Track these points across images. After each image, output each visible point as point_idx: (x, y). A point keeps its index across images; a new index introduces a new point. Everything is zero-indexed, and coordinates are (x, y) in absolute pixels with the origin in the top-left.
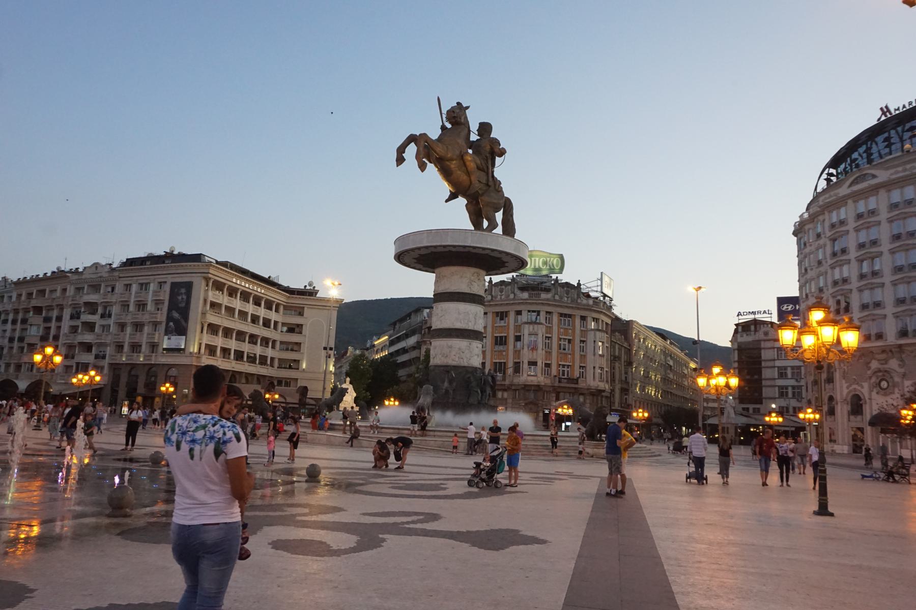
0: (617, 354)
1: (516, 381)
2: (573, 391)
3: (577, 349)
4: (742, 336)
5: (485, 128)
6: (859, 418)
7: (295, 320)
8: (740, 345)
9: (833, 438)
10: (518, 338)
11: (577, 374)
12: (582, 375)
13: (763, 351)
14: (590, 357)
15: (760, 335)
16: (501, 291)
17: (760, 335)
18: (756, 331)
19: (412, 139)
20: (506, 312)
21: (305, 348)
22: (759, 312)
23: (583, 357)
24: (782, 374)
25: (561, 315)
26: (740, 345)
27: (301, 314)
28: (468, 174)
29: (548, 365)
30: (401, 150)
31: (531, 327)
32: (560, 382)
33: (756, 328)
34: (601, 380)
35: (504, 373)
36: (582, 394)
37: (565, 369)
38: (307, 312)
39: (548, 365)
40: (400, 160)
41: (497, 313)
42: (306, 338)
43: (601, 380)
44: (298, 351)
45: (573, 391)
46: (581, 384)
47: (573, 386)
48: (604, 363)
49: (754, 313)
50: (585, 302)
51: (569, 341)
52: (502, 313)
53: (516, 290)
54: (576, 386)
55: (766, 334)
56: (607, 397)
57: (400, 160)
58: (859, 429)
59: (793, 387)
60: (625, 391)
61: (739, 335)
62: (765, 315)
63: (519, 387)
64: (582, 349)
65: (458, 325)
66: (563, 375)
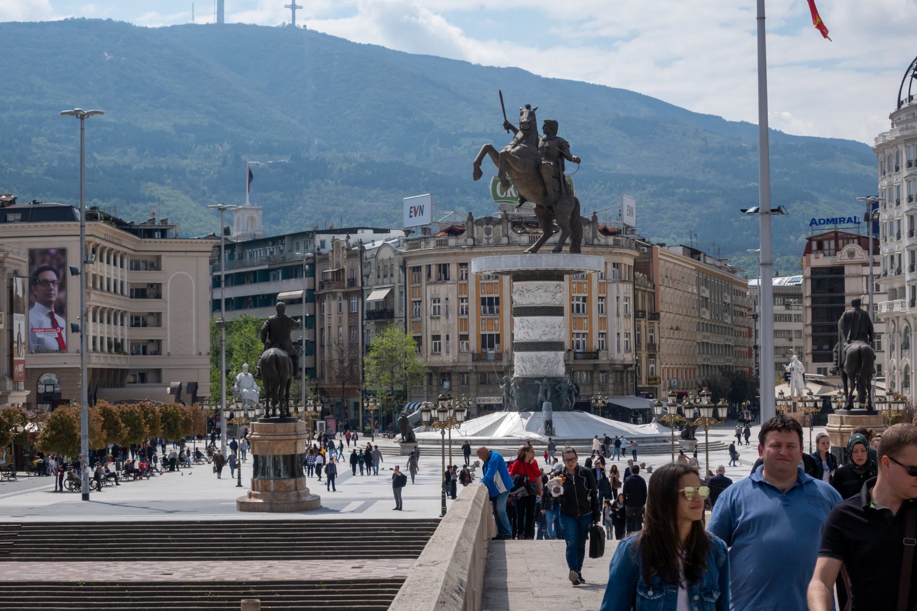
0: (640, 308)
3: (595, 310)
4: (817, 258)
5: (551, 127)
7: (146, 277)
8: (814, 270)
11: (595, 345)
12: (603, 346)
13: (847, 281)
14: (612, 320)
15: (842, 257)
16: (488, 232)
17: (842, 257)
18: (837, 249)
19: (489, 149)
21: (167, 320)
22: (842, 220)
23: (603, 321)
26: (814, 270)
27: (155, 265)
30: (478, 163)
32: (575, 358)
33: (837, 244)
34: (628, 350)
36: (603, 372)
37: (580, 339)
38: (165, 262)
40: (478, 174)
42: (166, 306)
43: (628, 350)
44: (158, 324)
46: (603, 359)
47: (592, 362)
48: (628, 325)
49: (833, 221)
50: (602, 239)
51: (584, 299)
54: (596, 362)
55: (851, 254)
56: (632, 371)
57: (478, 174)
60: (652, 356)
61: (812, 256)
62: (851, 225)
64: (601, 309)
65: (544, 339)
66: (578, 347)
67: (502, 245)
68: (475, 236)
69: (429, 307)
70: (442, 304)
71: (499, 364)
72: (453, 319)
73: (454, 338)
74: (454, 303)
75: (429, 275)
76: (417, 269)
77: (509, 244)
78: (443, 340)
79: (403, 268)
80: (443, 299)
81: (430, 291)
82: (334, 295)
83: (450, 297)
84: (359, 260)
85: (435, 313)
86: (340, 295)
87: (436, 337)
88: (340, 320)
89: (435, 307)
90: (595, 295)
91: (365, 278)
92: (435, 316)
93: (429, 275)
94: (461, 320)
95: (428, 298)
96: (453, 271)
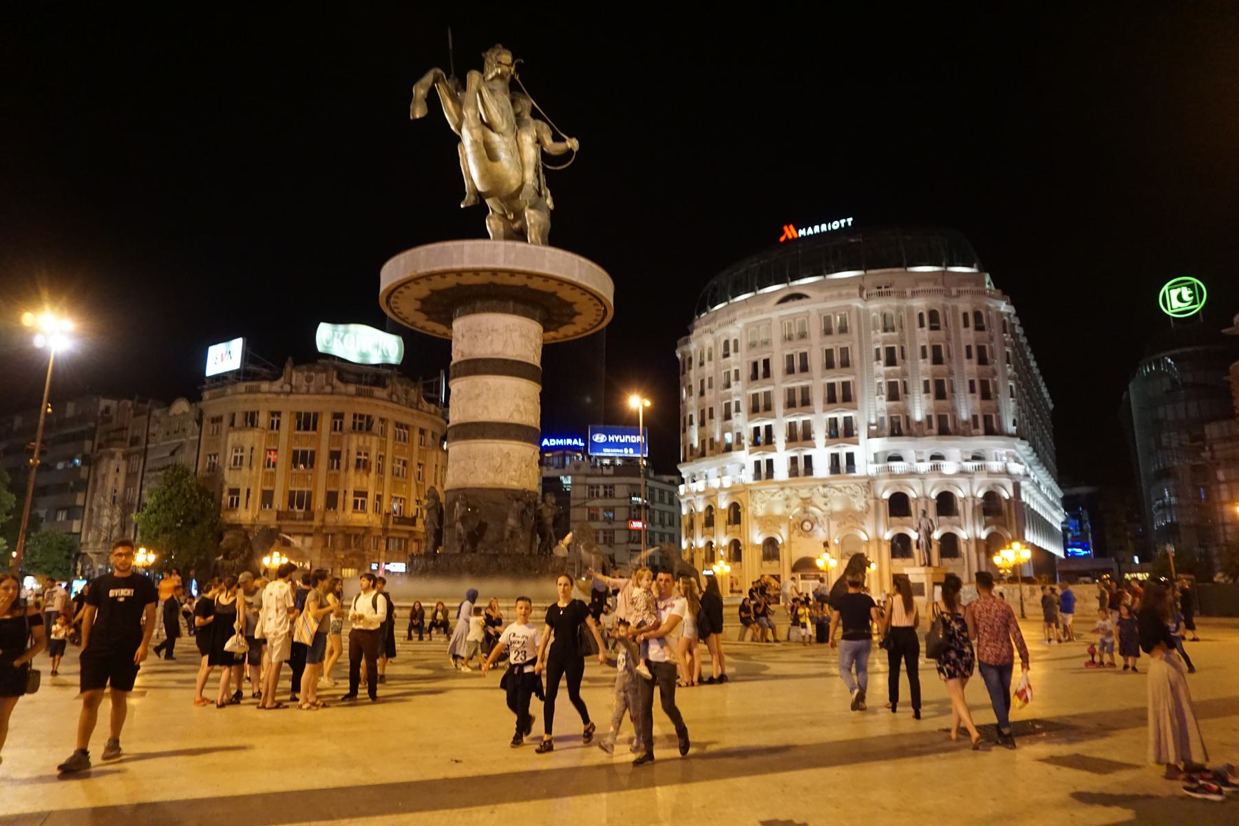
1: (330, 519)
2: (407, 536)
6: (775, 563)
9: (736, 588)
10: (335, 456)
16: (309, 379)
20: (316, 415)
24: (593, 517)
25: (399, 425)
28: (522, 166)
29: (379, 498)
31: (361, 439)
35: (308, 507)
39: (379, 498)
41: (299, 415)
45: (407, 536)
52: (307, 415)
53: (335, 381)
58: (773, 576)
59: (605, 531)
63: (334, 531)
67: (325, 394)
68: (294, 383)
69: (230, 456)
70: (246, 454)
71: (309, 523)
72: (258, 471)
73: (256, 497)
74: (260, 454)
75: (232, 424)
76: (217, 420)
77: (332, 393)
78: (243, 496)
79: (199, 422)
80: (247, 447)
81: (233, 438)
82: (112, 456)
83: (256, 447)
84: (145, 417)
85: (235, 463)
86: (119, 454)
87: (235, 492)
88: (116, 480)
89: (236, 458)
90: (415, 463)
91: (151, 438)
92: (238, 462)
93: (232, 424)
94: (266, 474)
95: (229, 447)
96: (263, 419)
